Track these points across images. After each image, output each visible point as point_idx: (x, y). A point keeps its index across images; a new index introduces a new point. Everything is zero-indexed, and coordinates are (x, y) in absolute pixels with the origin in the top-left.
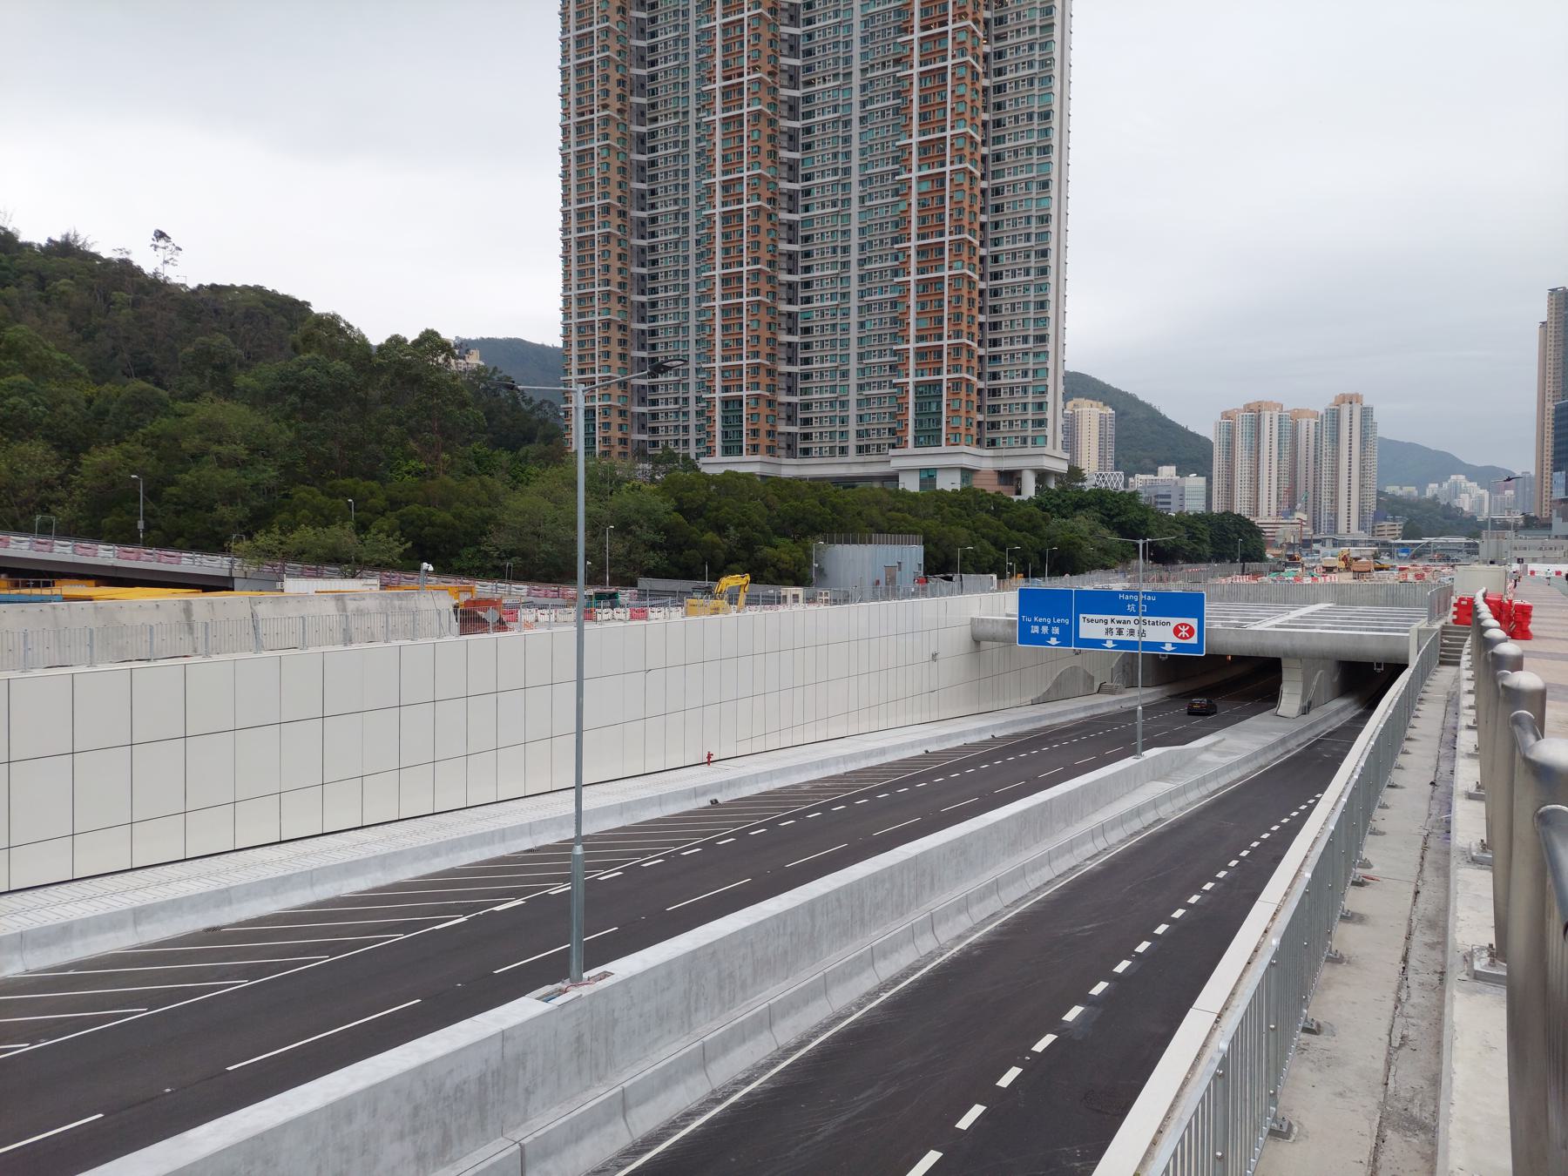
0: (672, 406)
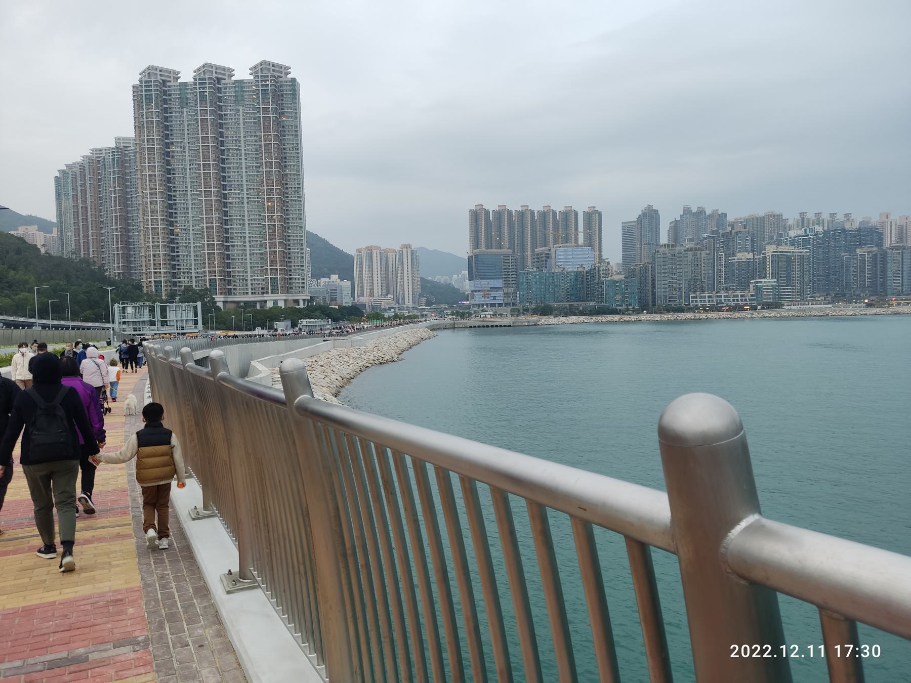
0: (186, 279)
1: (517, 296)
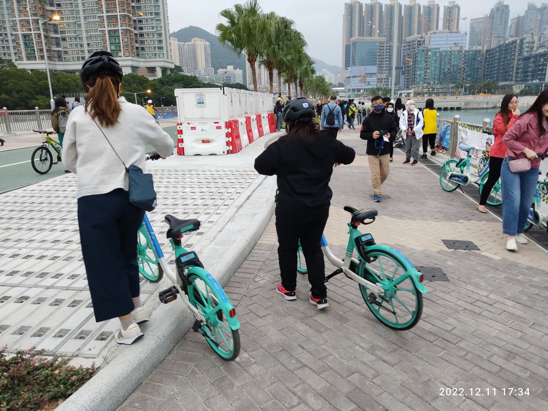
1: (388, 82)
